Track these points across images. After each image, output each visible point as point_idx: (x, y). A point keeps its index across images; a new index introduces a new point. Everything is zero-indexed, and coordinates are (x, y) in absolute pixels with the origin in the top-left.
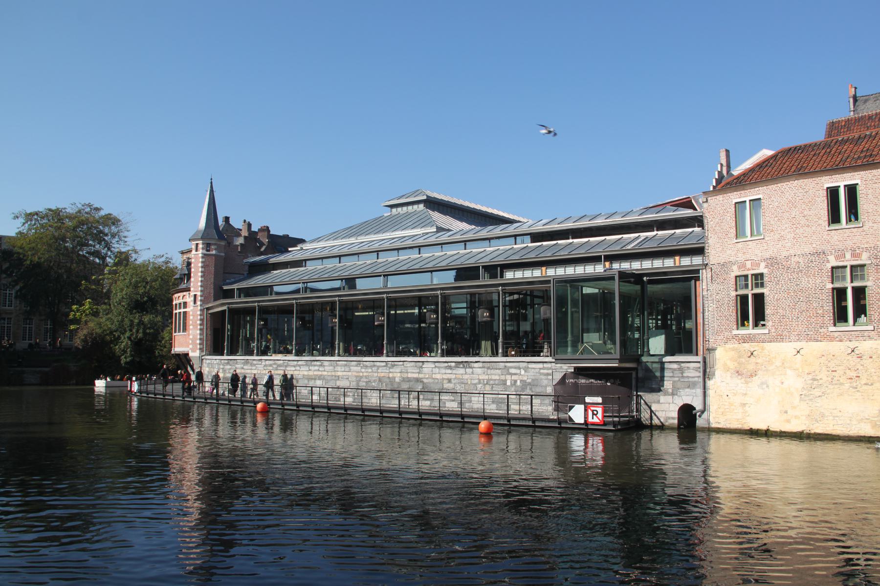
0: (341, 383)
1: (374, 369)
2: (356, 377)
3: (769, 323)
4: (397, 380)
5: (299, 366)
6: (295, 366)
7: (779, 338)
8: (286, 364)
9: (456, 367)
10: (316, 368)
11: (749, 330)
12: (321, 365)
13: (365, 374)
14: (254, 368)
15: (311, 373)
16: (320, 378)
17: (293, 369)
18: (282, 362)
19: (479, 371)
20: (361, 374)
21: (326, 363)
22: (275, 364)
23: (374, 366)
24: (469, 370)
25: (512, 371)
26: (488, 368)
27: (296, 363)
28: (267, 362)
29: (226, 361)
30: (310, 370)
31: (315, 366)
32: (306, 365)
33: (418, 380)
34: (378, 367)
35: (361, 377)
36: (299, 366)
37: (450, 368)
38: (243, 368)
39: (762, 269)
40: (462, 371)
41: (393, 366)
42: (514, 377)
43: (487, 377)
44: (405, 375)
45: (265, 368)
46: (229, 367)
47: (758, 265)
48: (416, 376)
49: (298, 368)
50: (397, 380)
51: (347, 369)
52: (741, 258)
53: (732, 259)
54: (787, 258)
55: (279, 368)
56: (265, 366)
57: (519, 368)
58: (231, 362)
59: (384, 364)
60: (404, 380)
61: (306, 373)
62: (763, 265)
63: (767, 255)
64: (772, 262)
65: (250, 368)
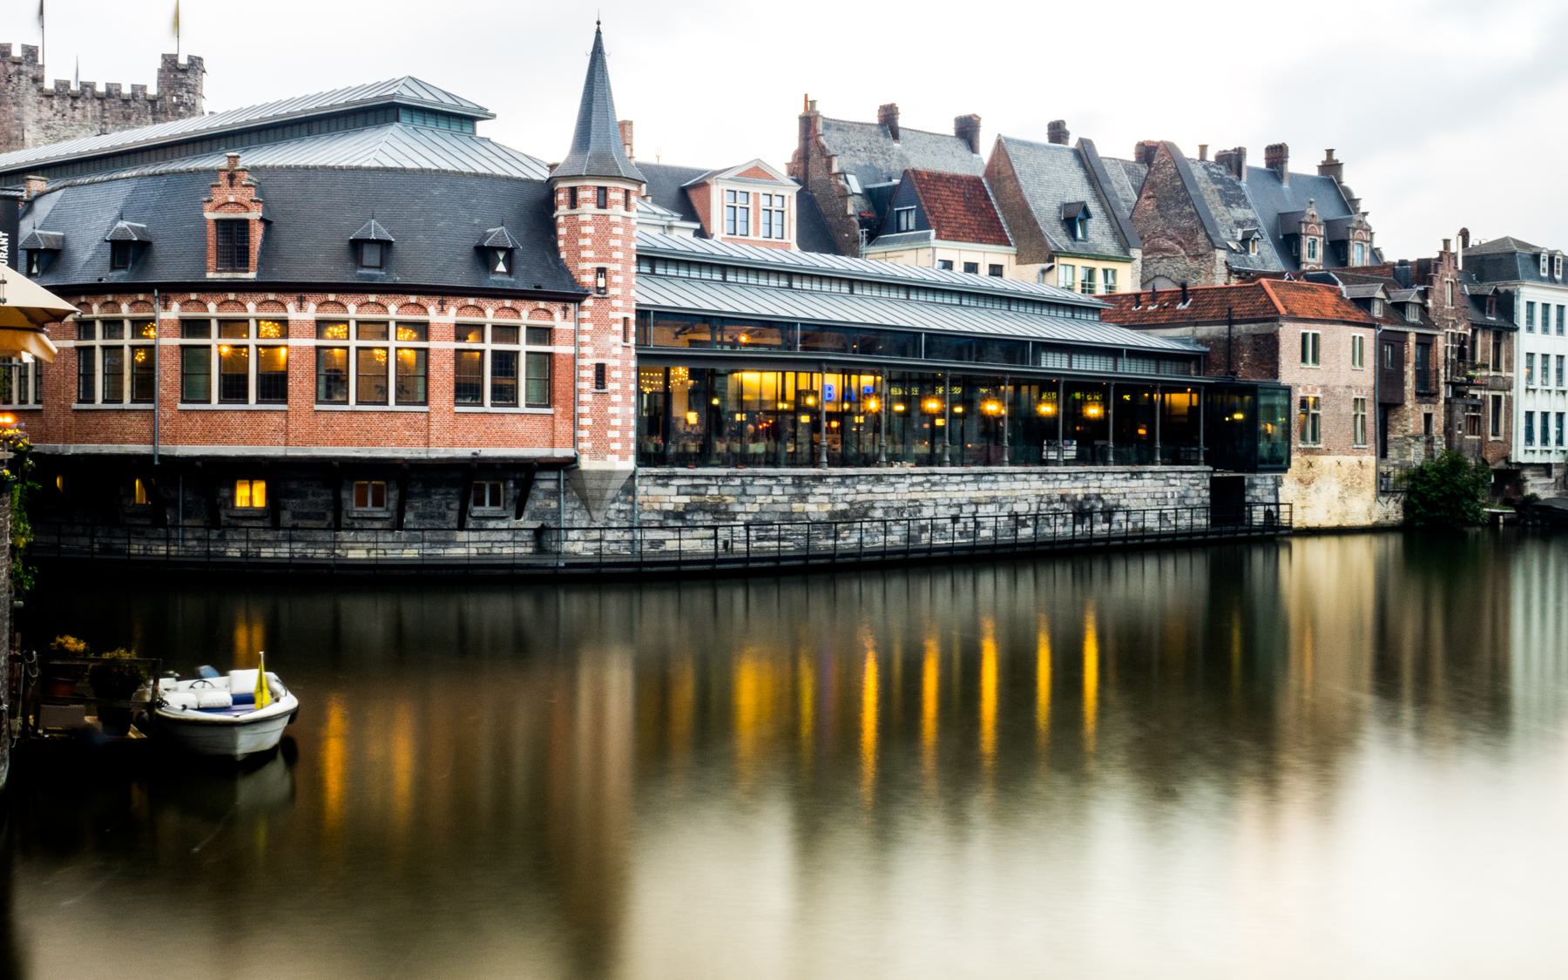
0: (1021, 508)
1: (1057, 483)
2: (1037, 496)
3: (1322, 440)
4: (1079, 498)
5: (965, 482)
6: (957, 484)
7: (1328, 452)
8: (944, 481)
9: (1131, 478)
10: (988, 485)
11: (1310, 445)
12: (993, 481)
13: (1047, 492)
14: (892, 489)
15: (979, 494)
16: (993, 500)
17: (956, 488)
18: (937, 477)
19: (1148, 482)
20: (1042, 493)
21: (1001, 478)
22: (928, 481)
23: (1056, 479)
24: (1140, 482)
25: (1172, 482)
26: (1155, 479)
27: (959, 478)
28: (916, 479)
29: (839, 480)
30: (979, 489)
31: (986, 482)
32: (975, 481)
33: (1099, 497)
34: (1062, 480)
35: (1042, 496)
36: (965, 482)
37: (1126, 479)
38: (870, 492)
39: (1318, 394)
40: (1134, 483)
41: (1076, 478)
42: (1173, 489)
43: (1154, 490)
44: (1086, 492)
45: (911, 489)
46: (842, 490)
47: (1316, 390)
48: (1096, 491)
49: (962, 487)
50: (1079, 498)
51: (1026, 485)
52: (1303, 382)
53: (1298, 381)
54: (1334, 388)
55: (933, 489)
56: (912, 485)
57: (1175, 478)
58: (848, 481)
59: (1066, 477)
60: (1087, 498)
61: (973, 494)
62: (1319, 390)
63: (1322, 382)
64: (1324, 388)
65: (884, 490)
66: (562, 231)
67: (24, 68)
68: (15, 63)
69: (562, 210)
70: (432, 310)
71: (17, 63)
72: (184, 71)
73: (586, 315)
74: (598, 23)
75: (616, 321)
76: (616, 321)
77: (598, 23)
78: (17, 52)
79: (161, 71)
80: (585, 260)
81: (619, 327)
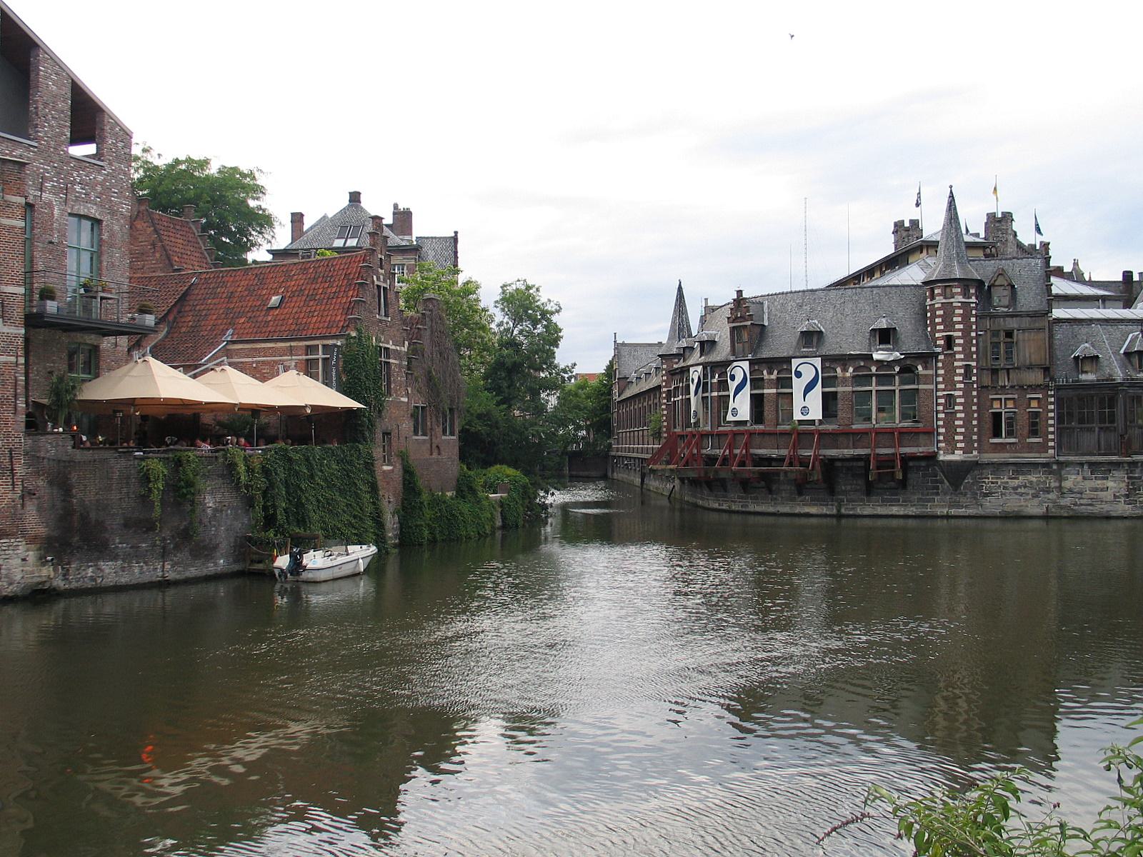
66: (929, 315)
67: (911, 233)
68: (906, 231)
69: (928, 302)
70: (839, 370)
71: (907, 230)
72: (1000, 221)
73: (940, 365)
74: (951, 187)
75: (960, 367)
76: (960, 367)
77: (951, 187)
78: (907, 224)
79: (986, 224)
80: (940, 331)
81: (962, 371)
